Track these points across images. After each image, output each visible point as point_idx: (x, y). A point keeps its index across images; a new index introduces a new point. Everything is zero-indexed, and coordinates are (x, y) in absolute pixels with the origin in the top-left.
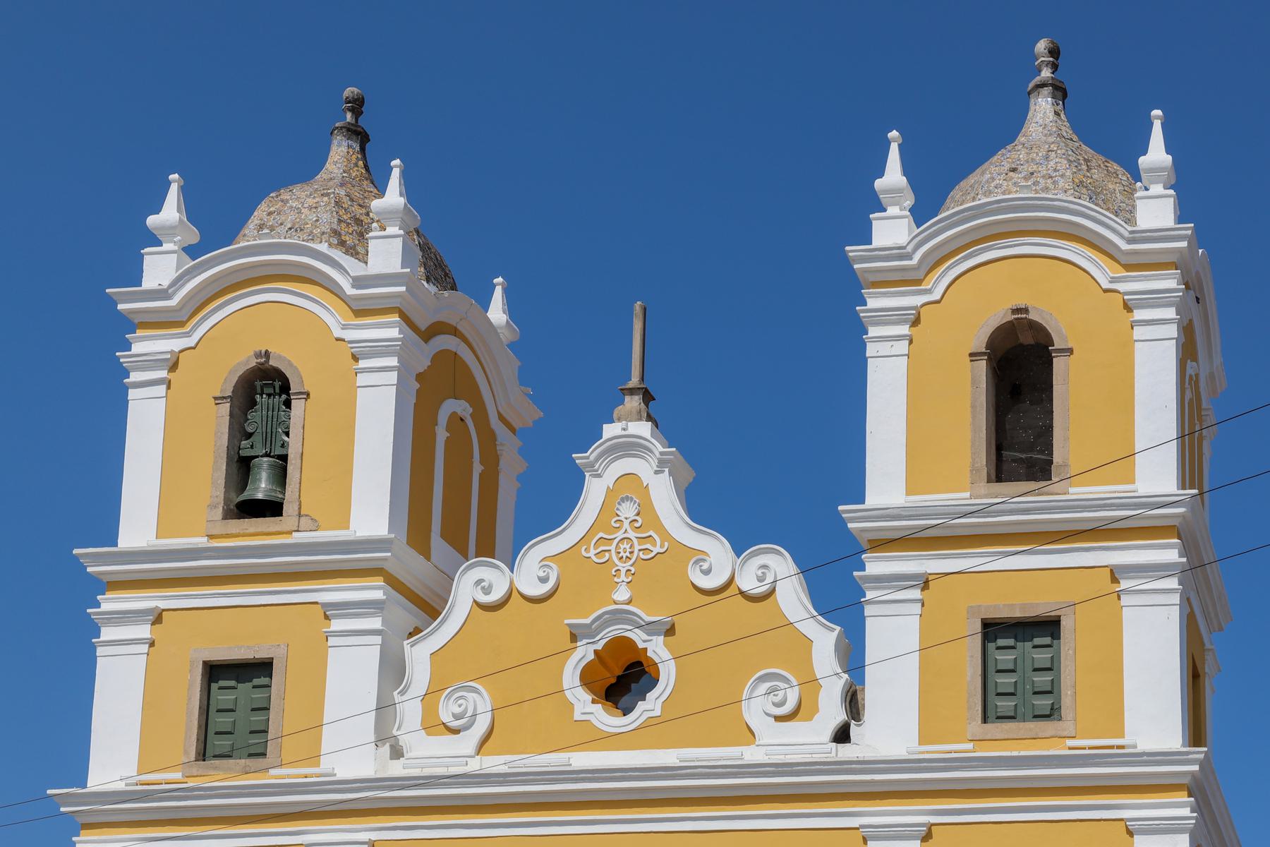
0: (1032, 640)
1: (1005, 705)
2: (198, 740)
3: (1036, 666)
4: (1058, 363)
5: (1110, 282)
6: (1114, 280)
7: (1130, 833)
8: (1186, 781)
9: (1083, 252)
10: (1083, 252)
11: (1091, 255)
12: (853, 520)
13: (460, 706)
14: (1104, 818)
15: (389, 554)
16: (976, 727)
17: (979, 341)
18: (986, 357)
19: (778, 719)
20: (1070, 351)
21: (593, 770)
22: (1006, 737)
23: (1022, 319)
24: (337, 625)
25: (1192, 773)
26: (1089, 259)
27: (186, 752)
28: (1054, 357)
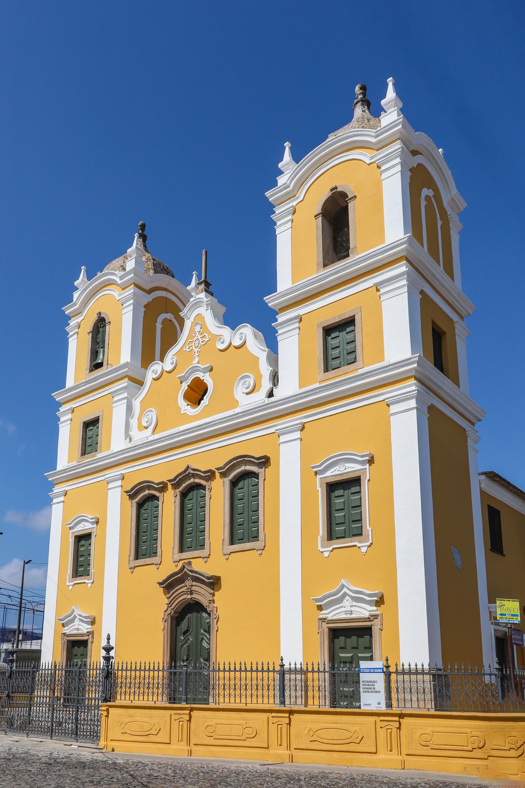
0: (345, 330)
1: (336, 363)
2: (82, 449)
3: (348, 341)
4: (351, 205)
5: (370, 159)
6: (372, 158)
7: (388, 405)
8: (413, 373)
9: (358, 152)
10: (358, 152)
11: (361, 152)
12: (270, 302)
13: (147, 418)
14: (376, 401)
15: (127, 369)
16: (322, 375)
17: (318, 209)
18: (321, 215)
19: (247, 394)
20: (355, 197)
21: (183, 431)
22: (334, 376)
23: (334, 192)
24: (116, 399)
25: (415, 369)
26: (361, 154)
27: (79, 454)
28: (349, 203)
